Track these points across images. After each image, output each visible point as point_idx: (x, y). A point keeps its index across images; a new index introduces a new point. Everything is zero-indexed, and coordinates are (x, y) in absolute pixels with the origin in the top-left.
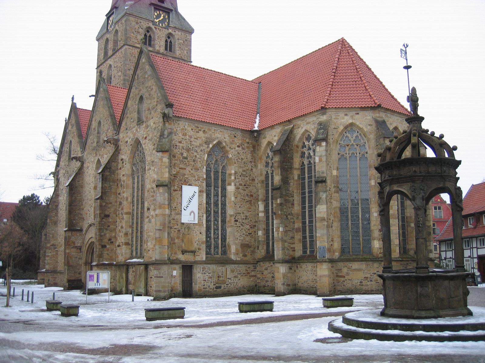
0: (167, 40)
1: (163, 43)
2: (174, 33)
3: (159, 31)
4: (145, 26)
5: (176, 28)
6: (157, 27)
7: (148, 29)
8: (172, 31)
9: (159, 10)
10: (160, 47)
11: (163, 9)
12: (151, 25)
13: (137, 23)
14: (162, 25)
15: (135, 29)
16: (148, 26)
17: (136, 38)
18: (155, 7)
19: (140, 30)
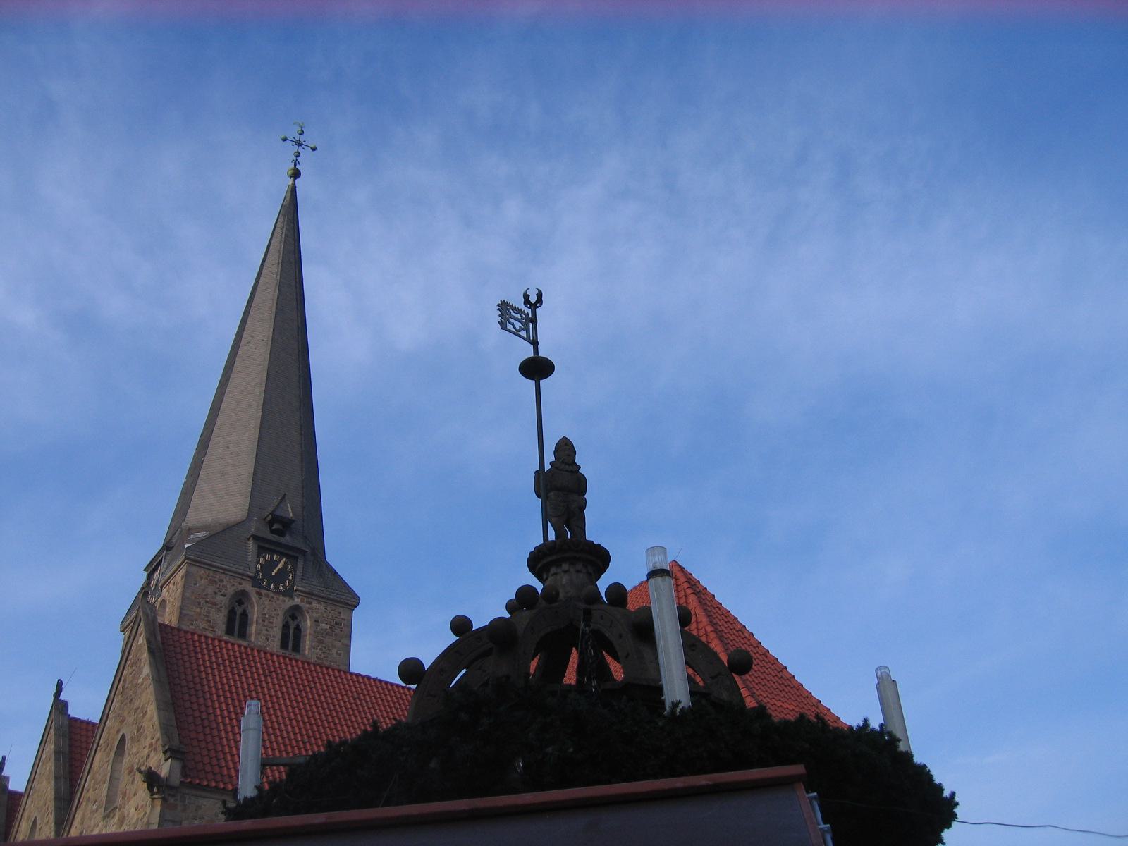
0: (287, 622)
1: (277, 632)
2: (305, 606)
3: (267, 602)
4: (233, 589)
5: (313, 595)
6: (264, 592)
7: (240, 598)
8: (301, 601)
9: (272, 552)
10: (267, 639)
11: (282, 550)
12: (247, 586)
13: (212, 582)
14: (277, 587)
15: (207, 595)
16: (240, 588)
17: (207, 616)
18: (261, 544)
19: (219, 598)
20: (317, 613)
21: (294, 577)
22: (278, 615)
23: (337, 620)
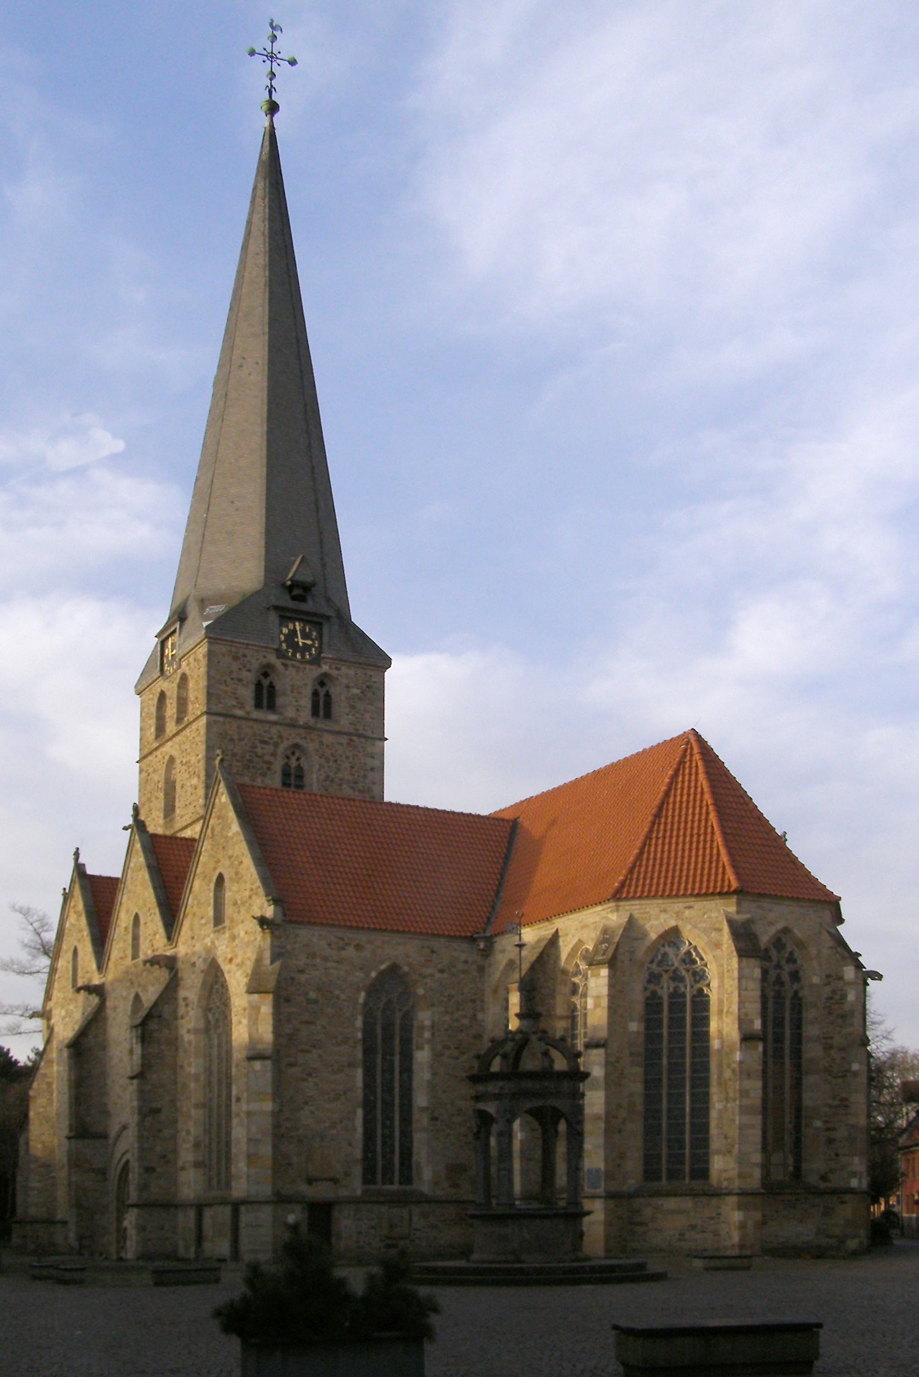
1: (306, 703)
2: (334, 673)
5: (341, 660)
6: (289, 662)
8: (330, 668)
10: (298, 710)
12: (272, 659)
15: (231, 672)
16: (265, 661)
18: (283, 614)
20: (347, 678)
21: (321, 644)
22: (306, 685)
23: (368, 684)
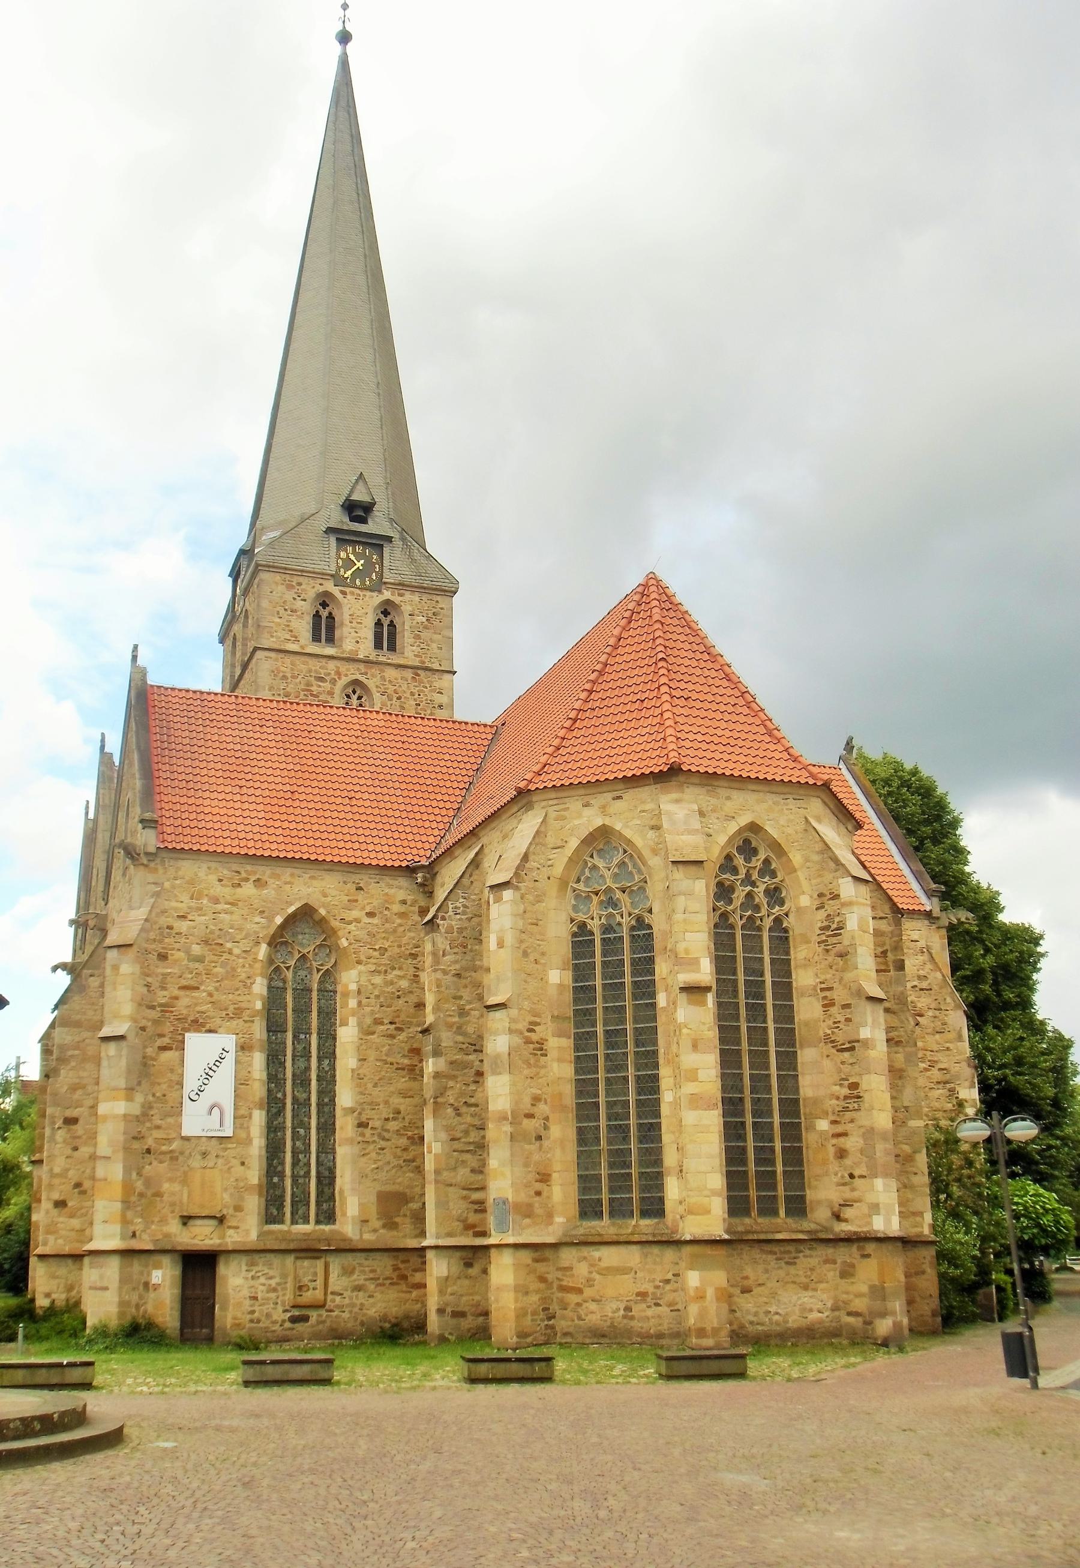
1: (368, 634)
2: (397, 599)
5: (404, 585)
6: (348, 590)
7: (325, 600)
12: (330, 586)
15: (285, 602)
16: (321, 589)
19: (299, 604)
